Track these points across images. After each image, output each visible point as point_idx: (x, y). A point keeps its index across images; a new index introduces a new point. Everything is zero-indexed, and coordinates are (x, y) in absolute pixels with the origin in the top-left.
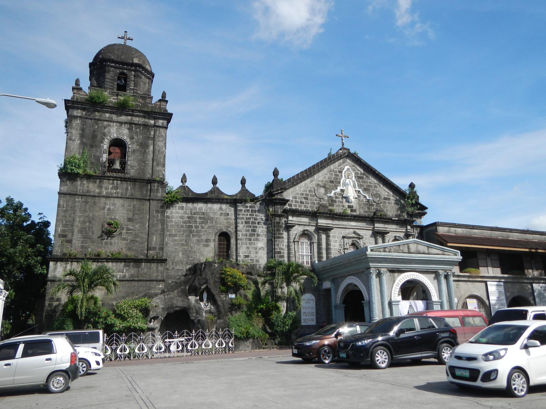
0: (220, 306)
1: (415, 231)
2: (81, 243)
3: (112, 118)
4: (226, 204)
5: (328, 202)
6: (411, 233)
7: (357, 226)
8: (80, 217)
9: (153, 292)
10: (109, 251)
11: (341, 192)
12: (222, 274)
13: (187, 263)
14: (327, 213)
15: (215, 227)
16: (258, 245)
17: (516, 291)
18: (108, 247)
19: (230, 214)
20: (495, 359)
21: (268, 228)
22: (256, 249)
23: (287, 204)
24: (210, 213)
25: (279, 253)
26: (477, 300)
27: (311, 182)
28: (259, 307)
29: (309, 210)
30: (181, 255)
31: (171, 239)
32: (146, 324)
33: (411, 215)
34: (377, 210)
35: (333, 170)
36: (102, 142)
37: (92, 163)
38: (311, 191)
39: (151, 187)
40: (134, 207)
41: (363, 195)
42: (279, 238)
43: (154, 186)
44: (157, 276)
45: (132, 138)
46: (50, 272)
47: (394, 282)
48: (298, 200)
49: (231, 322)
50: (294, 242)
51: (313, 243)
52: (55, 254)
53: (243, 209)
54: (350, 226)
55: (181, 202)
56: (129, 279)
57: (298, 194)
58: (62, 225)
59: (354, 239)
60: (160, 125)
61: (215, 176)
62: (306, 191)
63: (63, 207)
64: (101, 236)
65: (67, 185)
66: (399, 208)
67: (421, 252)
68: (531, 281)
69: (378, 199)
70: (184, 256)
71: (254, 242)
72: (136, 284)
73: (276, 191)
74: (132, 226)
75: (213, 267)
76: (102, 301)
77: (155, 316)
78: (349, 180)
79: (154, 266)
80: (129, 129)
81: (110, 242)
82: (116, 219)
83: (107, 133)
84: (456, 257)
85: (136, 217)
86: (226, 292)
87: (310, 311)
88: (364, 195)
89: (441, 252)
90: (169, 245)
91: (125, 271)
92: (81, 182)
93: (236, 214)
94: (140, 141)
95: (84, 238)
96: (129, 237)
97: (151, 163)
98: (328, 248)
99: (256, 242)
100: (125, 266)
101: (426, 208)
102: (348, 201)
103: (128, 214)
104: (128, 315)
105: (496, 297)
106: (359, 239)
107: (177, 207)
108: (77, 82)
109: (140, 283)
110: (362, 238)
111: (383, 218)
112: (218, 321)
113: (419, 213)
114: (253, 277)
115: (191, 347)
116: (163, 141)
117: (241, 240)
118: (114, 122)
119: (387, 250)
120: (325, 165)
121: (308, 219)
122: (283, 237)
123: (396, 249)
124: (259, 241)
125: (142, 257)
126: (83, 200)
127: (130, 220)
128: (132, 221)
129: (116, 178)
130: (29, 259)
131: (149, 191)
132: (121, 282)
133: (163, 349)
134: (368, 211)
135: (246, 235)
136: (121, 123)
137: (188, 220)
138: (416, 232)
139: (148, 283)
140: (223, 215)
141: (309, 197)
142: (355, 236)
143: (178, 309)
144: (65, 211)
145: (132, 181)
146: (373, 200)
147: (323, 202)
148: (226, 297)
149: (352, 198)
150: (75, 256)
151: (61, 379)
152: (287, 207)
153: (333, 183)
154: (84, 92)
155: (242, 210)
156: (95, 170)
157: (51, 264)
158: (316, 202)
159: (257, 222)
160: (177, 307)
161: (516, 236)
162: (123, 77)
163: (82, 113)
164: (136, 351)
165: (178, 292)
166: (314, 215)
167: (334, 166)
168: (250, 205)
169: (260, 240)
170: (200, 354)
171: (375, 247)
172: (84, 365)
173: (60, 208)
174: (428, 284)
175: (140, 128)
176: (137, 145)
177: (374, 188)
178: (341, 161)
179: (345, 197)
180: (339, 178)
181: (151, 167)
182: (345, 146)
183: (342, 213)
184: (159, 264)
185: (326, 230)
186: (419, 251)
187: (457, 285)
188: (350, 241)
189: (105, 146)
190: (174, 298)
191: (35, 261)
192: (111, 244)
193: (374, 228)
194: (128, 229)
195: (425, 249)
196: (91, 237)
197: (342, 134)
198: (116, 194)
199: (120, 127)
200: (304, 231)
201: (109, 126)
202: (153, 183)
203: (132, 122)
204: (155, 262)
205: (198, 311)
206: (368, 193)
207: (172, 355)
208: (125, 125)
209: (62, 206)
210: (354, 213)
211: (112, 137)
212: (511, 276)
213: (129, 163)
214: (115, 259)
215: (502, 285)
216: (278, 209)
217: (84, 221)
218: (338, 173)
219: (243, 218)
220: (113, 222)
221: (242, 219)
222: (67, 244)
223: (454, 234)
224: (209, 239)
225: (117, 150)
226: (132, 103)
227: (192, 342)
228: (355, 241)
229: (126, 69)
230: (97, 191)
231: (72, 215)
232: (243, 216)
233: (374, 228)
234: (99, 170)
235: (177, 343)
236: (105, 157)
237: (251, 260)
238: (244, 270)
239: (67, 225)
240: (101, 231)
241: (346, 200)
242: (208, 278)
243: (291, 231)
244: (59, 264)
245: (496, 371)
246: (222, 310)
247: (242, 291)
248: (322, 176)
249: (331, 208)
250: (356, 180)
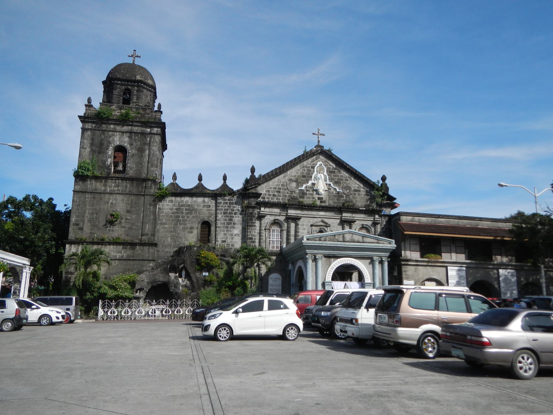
0: (194, 282)
1: (383, 220)
2: (90, 230)
3: (116, 129)
4: (208, 198)
5: (299, 194)
6: (378, 222)
7: (325, 216)
8: (89, 210)
9: (144, 269)
10: (111, 236)
11: (312, 185)
12: (199, 256)
13: (174, 247)
14: (296, 205)
15: (198, 217)
16: (234, 232)
17: (479, 275)
18: (110, 234)
19: (211, 206)
20: (214, 318)
21: (243, 218)
22: (232, 235)
23: (261, 197)
24: (194, 205)
25: (251, 239)
26: (436, 283)
27: (284, 177)
28: (227, 284)
29: (281, 202)
30: (169, 239)
31: (162, 227)
32: (132, 294)
33: (381, 205)
34: (346, 201)
35: (306, 166)
36: (107, 149)
37: (99, 166)
38: (284, 185)
39: (145, 185)
40: (132, 201)
41: (333, 188)
42: (252, 226)
43: (149, 184)
44: (148, 256)
45: (131, 144)
46: (66, 253)
47: (330, 266)
48: (271, 193)
49: (202, 295)
50: (265, 229)
51: (283, 230)
52: (70, 238)
53: (222, 202)
54: (318, 215)
55: (170, 196)
56: (126, 258)
57: (271, 188)
58: (76, 216)
59: (321, 227)
60: (155, 132)
61: (200, 173)
62: (279, 185)
63: (77, 202)
64: (105, 225)
65: (79, 185)
66: (369, 198)
67: (356, 241)
68: (497, 267)
69: (348, 191)
70: (172, 240)
71: (230, 229)
72: (131, 262)
73: (250, 186)
74: (130, 216)
75: (193, 250)
76: (105, 275)
77: (140, 287)
78: (321, 174)
79: (146, 248)
80: (129, 137)
81: (112, 229)
82: (117, 211)
83: (112, 141)
84: (390, 245)
85: (133, 209)
86: (201, 270)
87: (277, 288)
88: (335, 187)
89: (375, 241)
90: (160, 232)
91: (123, 252)
92: (91, 182)
93: (216, 206)
94: (138, 147)
95: (92, 226)
96: (127, 226)
97: (146, 164)
98: (296, 235)
99: (232, 229)
100: (123, 248)
101: (395, 199)
102: (318, 193)
103: (127, 207)
104: (118, 287)
105: (456, 281)
106: (327, 227)
107: (168, 201)
108: (89, 100)
109: (135, 262)
110: (329, 226)
111: (350, 209)
112: (192, 293)
113: (388, 203)
114: (226, 259)
115: (166, 312)
116: (157, 146)
117: (219, 227)
118: (117, 132)
119: (322, 239)
120: (298, 162)
121: (279, 210)
122: (255, 226)
123: (331, 238)
124: (235, 228)
125: (137, 241)
126: (92, 196)
127: (128, 212)
128: (130, 213)
129: (118, 178)
130: (46, 243)
131: (144, 188)
132: (120, 261)
133: (143, 314)
134: (337, 202)
135: (224, 224)
136: (123, 132)
137: (176, 211)
138: (384, 221)
139: (141, 262)
140: (206, 206)
141: (281, 190)
142: (323, 224)
143: (160, 283)
144: (78, 205)
145: (130, 180)
146: (343, 192)
147: (294, 195)
148: (200, 275)
149: (321, 191)
150: (85, 240)
151: (10, 323)
152: (260, 199)
153: (305, 178)
154: (94, 108)
155: (221, 202)
156: (101, 172)
157: (67, 246)
158: (287, 195)
159: (234, 212)
160: (159, 281)
161: (486, 224)
162: (128, 92)
163: (92, 126)
164: (123, 314)
165: (160, 270)
166: (284, 207)
167: (307, 163)
168: (229, 198)
169: (236, 227)
170: (173, 318)
171: (311, 237)
172: (45, 318)
173: (74, 203)
174: (362, 268)
175: (138, 136)
176: (136, 150)
177: (345, 181)
178: (315, 157)
179: (316, 191)
180: (311, 173)
181: (147, 168)
182: (320, 144)
183: (311, 204)
184: (151, 247)
185: (296, 219)
186: (354, 240)
188: (318, 229)
189: (110, 151)
190: (157, 274)
191: (51, 245)
192: (113, 231)
193: (341, 217)
194: (127, 219)
195: (360, 239)
196: (98, 225)
197: (318, 132)
198: (118, 191)
199: (122, 135)
200: (275, 220)
201: (113, 135)
202: (147, 181)
203: (132, 131)
204: (147, 246)
205: (177, 285)
206: (338, 186)
207: (150, 318)
208: (126, 134)
209: (75, 201)
210: (323, 204)
211: (115, 144)
212: (473, 262)
213: (129, 165)
214: (115, 243)
215: (464, 270)
216: (252, 201)
217: (93, 213)
218: (310, 169)
219: (222, 209)
220: (114, 213)
221: (220, 210)
222: (79, 231)
223: (417, 223)
224: (193, 227)
225: (121, 155)
226: (132, 114)
227: (167, 309)
228: (322, 228)
229: (130, 86)
230: (103, 188)
231: (83, 208)
232: (222, 208)
233: (341, 217)
234: (105, 172)
235: (155, 309)
236: (110, 161)
237: (227, 244)
238: (219, 253)
239: (79, 216)
240: (105, 220)
241: (317, 192)
242: (185, 259)
243: (263, 221)
244: (73, 246)
245: (210, 325)
246: (196, 285)
247: (215, 270)
248: (295, 171)
249: (301, 200)
250: (328, 175)
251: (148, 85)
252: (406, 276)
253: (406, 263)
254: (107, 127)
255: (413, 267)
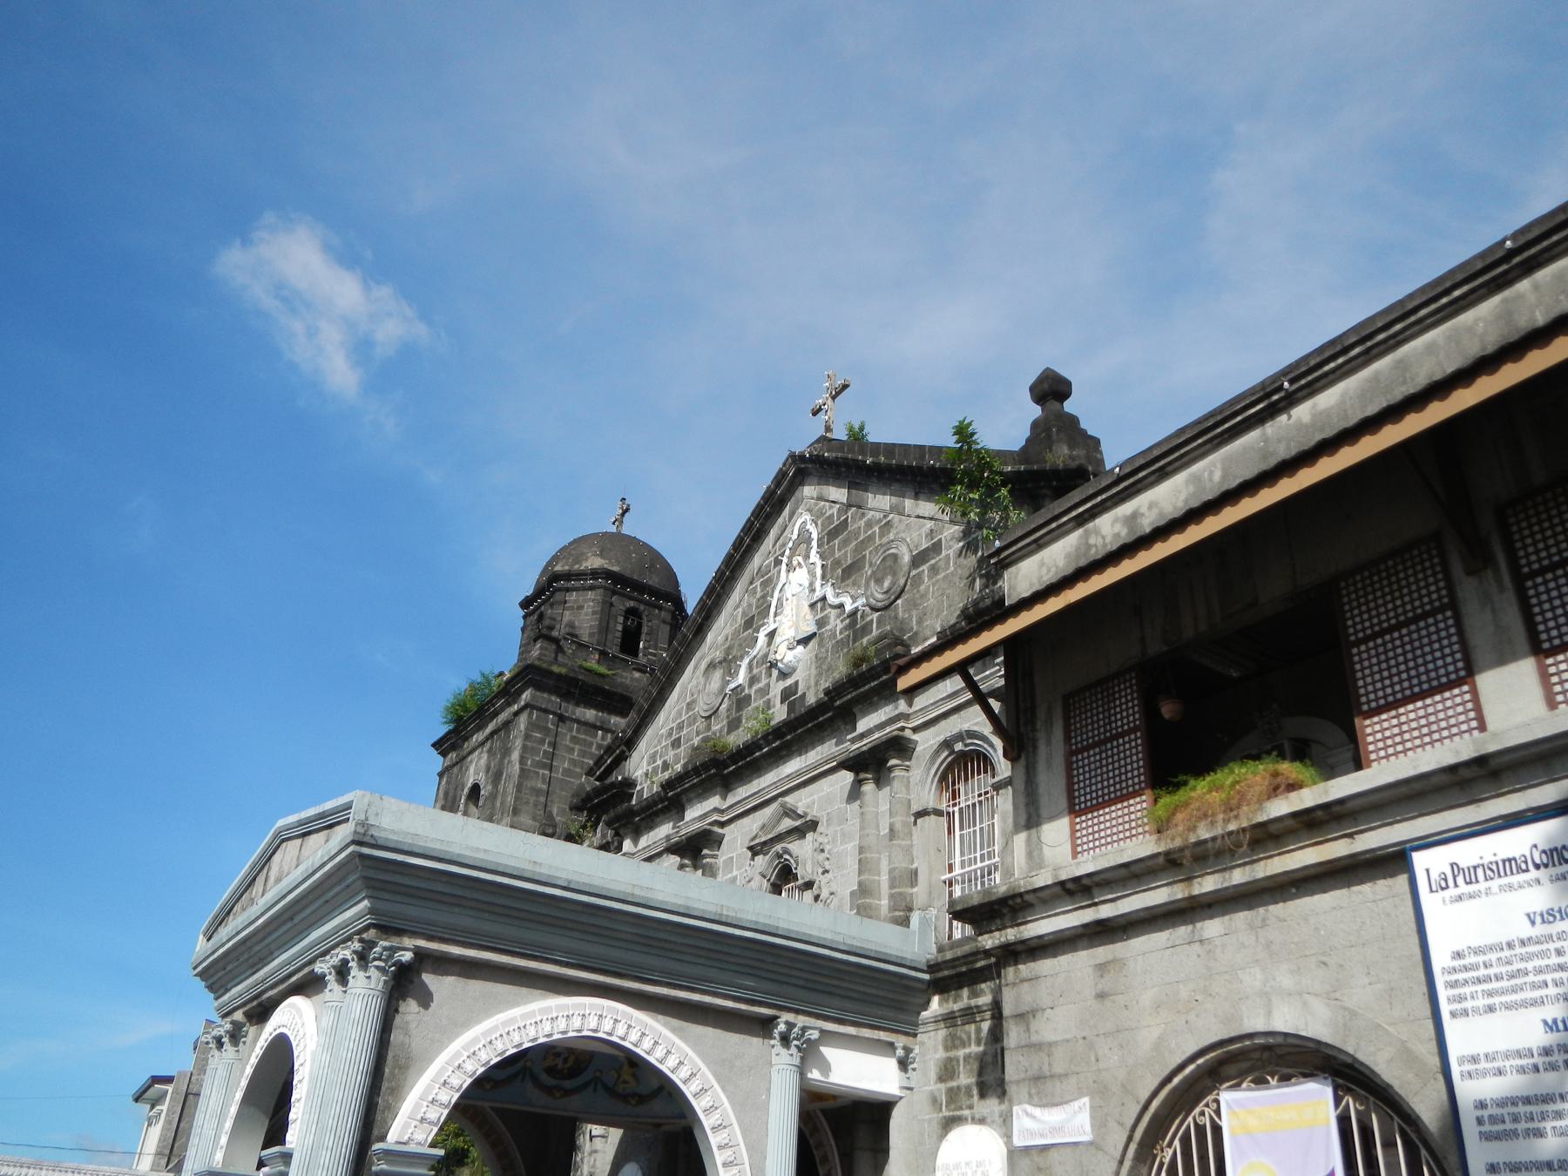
27: (696, 668)
60: (523, 703)
69: (886, 584)
136: (482, 744)
146: (868, 605)
149: (786, 655)
187: (1102, 968)
201: (471, 761)
229: (544, 602)
250: (822, 557)
251: (580, 575)
252: (1035, 1062)
253: (1011, 934)
254: (468, 747)
255: (1078, 964)
